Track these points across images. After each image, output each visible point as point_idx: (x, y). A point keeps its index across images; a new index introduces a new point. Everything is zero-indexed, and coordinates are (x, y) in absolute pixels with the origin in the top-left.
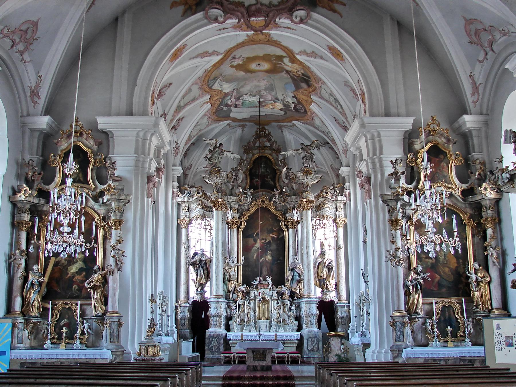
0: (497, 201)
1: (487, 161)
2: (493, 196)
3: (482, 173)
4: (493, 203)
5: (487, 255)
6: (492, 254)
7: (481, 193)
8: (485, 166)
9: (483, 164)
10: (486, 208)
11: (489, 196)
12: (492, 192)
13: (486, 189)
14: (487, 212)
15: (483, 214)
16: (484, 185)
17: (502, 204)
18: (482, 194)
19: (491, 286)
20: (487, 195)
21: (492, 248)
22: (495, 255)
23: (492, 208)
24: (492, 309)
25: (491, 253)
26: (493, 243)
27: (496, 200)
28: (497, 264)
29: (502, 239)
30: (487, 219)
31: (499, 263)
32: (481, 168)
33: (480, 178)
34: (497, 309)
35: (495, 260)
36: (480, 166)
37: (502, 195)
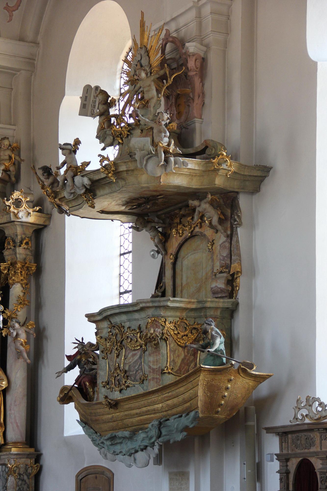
0: (38, 231)
1: (23, 145)
2: (31, 219)
3: (12, 169)
4: (29, 232)
5: (6, 336)
6: (17, 335)
7: (6, 211)
8: (19, 155)
9: (16, 149)
10: (14, 241)
11: (24, 219)
12: (30, 211)
13: (18, 203)
14: (14, 250)
15: (6, 253)
16: (16, 195)
17: (48, 237)
18: (8, 213)
19: (9, 398)
20: (20, 215)
21: (19, 323)
22: (23, 338)
23: (27, 243)
24: (6, 443)
25: (15, 334)
26: (21, 314)
27: (36, 227)
28: (25, 355)
29: (39, 307)
30: (13, 264)
31: (28, 354)
32: (10, 158)
33: (7, 178)
34: (15, 444)
35: (22, 348)
36: (8, 153)
37: (49, 217)
